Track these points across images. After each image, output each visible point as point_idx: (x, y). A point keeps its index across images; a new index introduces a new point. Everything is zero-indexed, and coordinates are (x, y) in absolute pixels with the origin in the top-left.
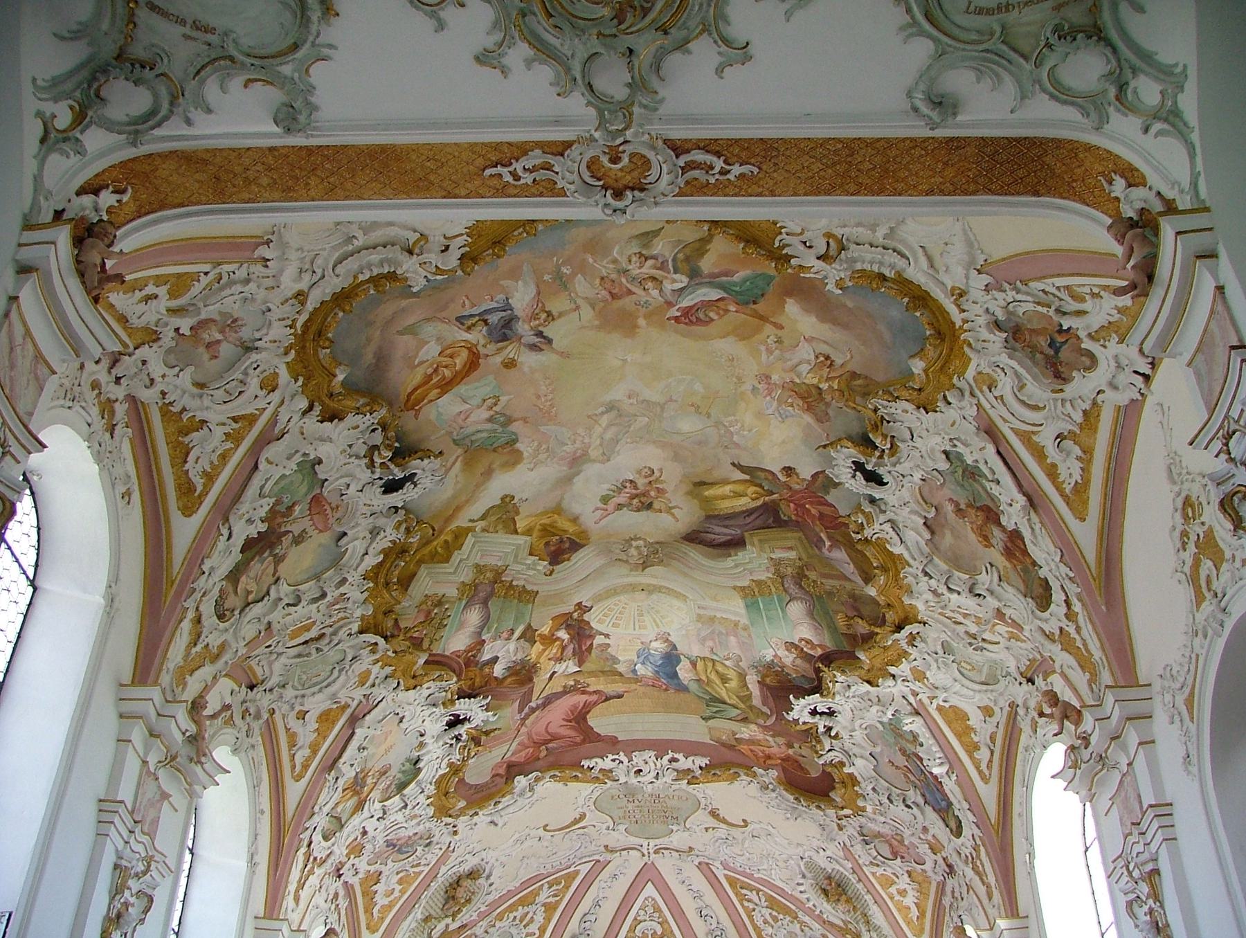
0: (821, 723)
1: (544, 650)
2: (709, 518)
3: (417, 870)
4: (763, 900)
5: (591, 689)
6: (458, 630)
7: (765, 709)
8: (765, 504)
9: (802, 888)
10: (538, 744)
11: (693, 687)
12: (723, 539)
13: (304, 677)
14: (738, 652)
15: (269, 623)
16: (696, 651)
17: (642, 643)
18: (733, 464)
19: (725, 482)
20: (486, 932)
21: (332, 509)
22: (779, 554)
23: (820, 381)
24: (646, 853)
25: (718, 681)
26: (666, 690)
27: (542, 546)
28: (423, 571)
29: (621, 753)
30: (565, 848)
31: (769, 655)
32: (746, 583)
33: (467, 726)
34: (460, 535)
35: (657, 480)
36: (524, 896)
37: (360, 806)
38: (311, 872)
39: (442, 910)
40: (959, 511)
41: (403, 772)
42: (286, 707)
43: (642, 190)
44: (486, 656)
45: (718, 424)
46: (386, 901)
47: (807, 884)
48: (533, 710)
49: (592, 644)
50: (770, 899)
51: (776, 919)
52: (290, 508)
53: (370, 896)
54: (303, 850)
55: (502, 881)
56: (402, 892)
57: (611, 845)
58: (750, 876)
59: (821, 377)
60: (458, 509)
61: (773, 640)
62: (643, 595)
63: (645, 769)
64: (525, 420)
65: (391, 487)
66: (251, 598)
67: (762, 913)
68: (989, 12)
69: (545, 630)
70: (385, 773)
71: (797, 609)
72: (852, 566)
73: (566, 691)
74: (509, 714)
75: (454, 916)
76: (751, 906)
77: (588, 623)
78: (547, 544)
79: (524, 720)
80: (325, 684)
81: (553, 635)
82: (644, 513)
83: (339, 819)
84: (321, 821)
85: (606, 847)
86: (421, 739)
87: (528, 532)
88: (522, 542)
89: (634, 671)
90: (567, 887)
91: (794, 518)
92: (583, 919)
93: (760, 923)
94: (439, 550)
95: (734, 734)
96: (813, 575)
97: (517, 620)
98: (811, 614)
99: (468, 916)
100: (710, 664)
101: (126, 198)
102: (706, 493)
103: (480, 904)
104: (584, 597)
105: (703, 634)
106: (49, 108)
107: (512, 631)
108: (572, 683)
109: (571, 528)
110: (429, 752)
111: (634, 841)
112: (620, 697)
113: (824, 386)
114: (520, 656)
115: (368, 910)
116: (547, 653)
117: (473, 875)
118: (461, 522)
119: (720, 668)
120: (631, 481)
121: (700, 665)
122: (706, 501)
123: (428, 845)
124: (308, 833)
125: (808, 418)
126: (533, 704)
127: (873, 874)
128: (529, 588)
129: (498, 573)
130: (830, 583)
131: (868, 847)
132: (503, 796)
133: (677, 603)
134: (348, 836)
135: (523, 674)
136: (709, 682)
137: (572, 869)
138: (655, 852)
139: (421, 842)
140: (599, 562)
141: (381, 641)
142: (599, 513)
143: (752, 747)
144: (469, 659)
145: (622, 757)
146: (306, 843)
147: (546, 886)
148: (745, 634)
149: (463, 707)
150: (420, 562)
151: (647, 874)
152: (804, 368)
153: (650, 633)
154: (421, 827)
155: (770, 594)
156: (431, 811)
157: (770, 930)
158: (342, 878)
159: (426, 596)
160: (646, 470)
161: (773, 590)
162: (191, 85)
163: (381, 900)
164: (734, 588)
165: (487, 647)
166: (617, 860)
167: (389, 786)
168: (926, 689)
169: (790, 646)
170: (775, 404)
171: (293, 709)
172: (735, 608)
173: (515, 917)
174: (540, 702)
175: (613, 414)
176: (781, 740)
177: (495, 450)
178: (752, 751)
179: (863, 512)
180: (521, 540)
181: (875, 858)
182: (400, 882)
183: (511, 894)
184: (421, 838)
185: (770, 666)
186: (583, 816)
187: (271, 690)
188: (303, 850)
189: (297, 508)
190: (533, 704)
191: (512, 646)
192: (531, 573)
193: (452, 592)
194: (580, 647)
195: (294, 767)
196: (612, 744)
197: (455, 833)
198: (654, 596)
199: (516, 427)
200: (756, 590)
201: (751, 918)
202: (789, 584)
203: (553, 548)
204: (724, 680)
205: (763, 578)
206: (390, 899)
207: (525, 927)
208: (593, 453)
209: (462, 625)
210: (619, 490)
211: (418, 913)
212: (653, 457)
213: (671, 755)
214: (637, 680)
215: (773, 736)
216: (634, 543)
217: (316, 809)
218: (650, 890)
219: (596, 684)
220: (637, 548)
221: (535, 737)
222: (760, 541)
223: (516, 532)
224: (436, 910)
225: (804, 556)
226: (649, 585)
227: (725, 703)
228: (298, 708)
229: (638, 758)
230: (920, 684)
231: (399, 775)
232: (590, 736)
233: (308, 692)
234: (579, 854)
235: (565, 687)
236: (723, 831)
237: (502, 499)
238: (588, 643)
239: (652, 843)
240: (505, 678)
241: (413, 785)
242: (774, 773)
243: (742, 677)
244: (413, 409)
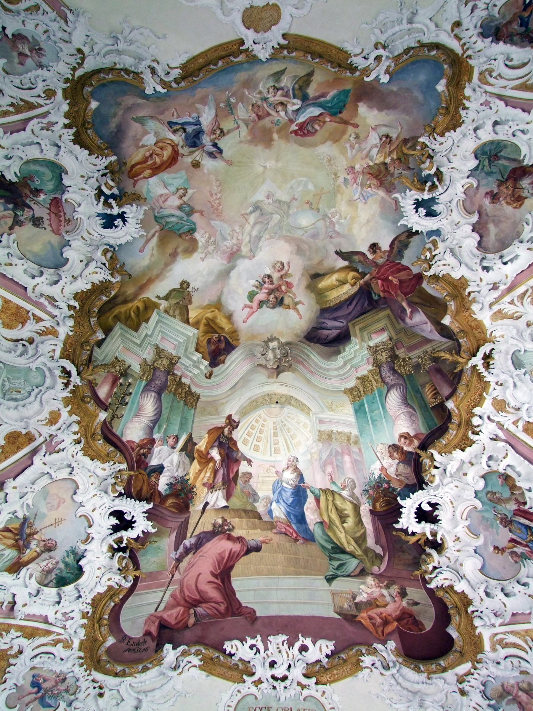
0: (426, 528)
1: (200, 471)
5: (236, 533)
6: (136, 415)
7: (379, 550)
8: (361, 288)
11: (317, 532)
12: (334, 333)
14: (351, 475)
17: (277, 472)
18: (337, 253)
19: (332, 271)
21: (66, 220)
23: (385, 158)
25: (337, 521)
26: (296, 540)
27: (205, 343)
29: (259, 637)
31: (375, 470)
32: (352, 383)
35: (286, 275)
40: (494, 197)
44: (154, 462)
48: (187, 551)
49: (237, 472)
59: (386, 153)
60: (150, 281)
61: (379, 449)
64: (202, 213)
72: (429, 323)
77: (235, 443)
78: (209, 341)
79: (179, 560)
81: (208, 453)
82: (278, 310)
88: (191, 334)
89: (270, 512)
91: (382, 295)
94: (132, 314)
96: (401, 353)
98: (405, 401)
100: (330, 498)
108: (220, 521)
114: (180, 473)
116: (202, 475)
119: (338, 502)
125: (381, 193)
126: (187, 542)
128: (194, 389)
133: (302, 418)
140: (246, 367)
142: (247, 310)
143: (370, 613)
144: (140, 455)
148: (355, 449)
152: (375, 151)
159: (116, 358)
160: (279, 264)
161: (374, 384)
164: (345, 392)
165: (156, 449)
168: (509, 416)
170: (360, 187)
174: (193, 541)
175: (258, 212)
176: (395, 589)
177: (180, 236)
178: (371, 618)
180: (191, 332)
185: (379, 483)
190: (187, 542)
192: (196, 371)
193: (136, 367)
199: (196, 217)
200: (361, 390)
203: (213, 347)
204: (343, 518)
205: (365, 372)
208: (245, 250)
210: (260, 286)
214: (272, 525)
215: (387, 587)
220: (273, 349)
221: (187, 593)
223: (187, 322)
225: (393, 334)
226: (282, 396)
227: (343, 551)
230: (504, 414)
231: (61, 565)
238: (235, 470)
240: (167, 496)
242: (392, 644)
243: (356, 508)
244: (133, 178)
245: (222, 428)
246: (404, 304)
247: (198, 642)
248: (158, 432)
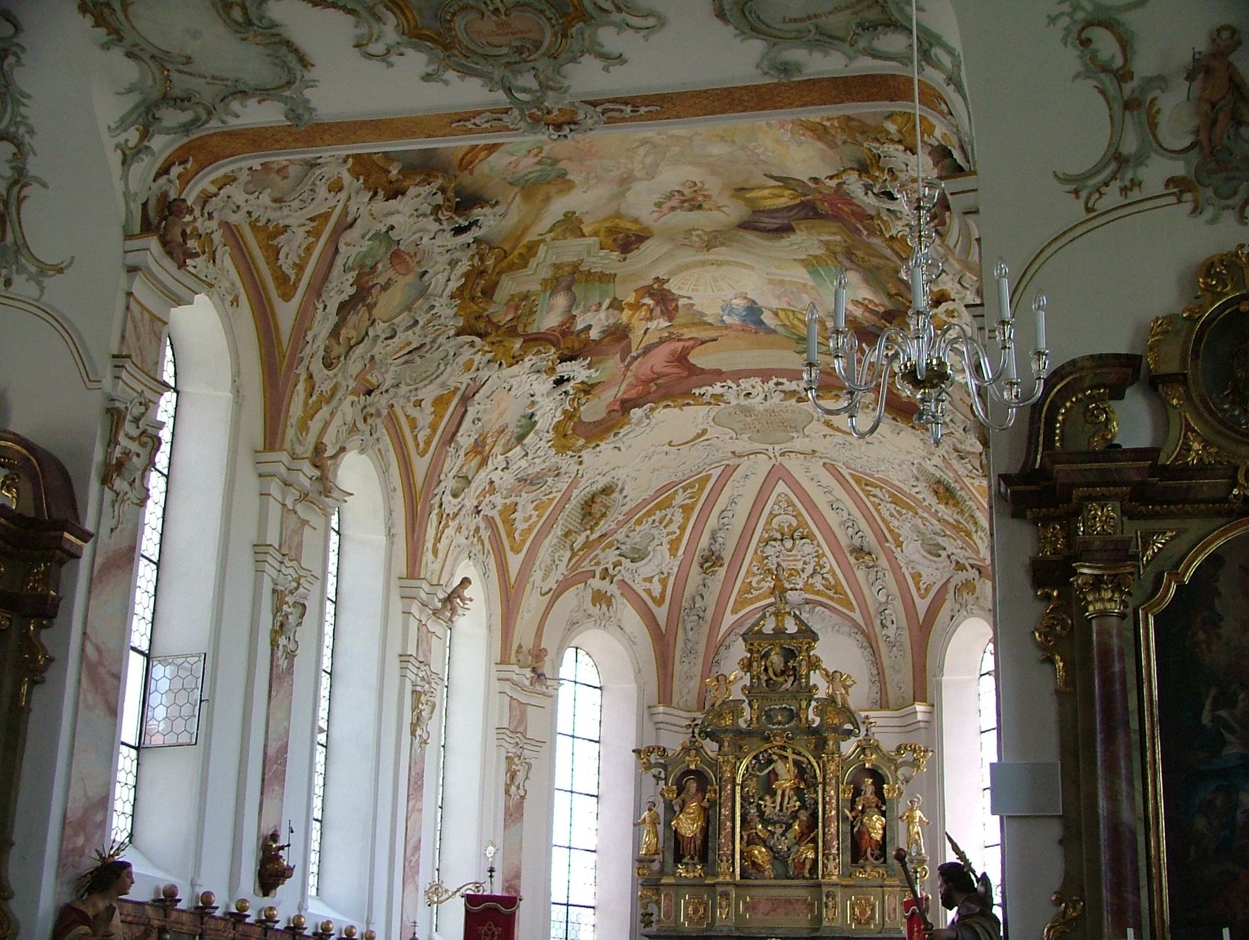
1: (633, 314)
2: (754, 212)
3: (550, 496)
4: (887, 496)
8: (802, 202)
9: (917, 490)
10: (647, 382)
11: (780, 329)
12: (774, 226)
13: (415, 375)
15: (373, 357)
16: (775, 304)
18: (766, 175)
19: (762, 188)
20: (627, 536)
22: (825, 238)
24: (772, 456)
28: (505, 279)
30: (693, 458)
32: (804, 257)
33: (572, 383)
34: (532, 248)
35: (701, 190)
36: (661, 500)
37: (484, 462)
38: (447, 526)
39: (581, 524)
41: (521, 426)
42: (402, 401)
43: (575, 123)
45: (743, 148)
46: (526, 526)
47: (921, 486)
48: (635, 358)
49: (677, 305)
50: (892, 495)
51: (900, 514)
52: (374, 268)
53: (509, 523)
54: (435, 511)
55: (635, 491)
56: (539, 516)
57: (738, 450)
58: (872, 476)
60: (526, 229)
62: (714, 267)
63: (754, 392)
64: (570, 159)
65: (459, 231)
66: (352, 343)
67: (887, 508)
68: (801, 20)
69: (631, 299)
70: (503, 431)
71: (853, 277)
73: (662, 341)
74: (613, 364)
75: (592, 529)
76: (877, 501)
77: (669, 291)
78: (615, 240)
80: (434, 376)
83: (466, 478)
84: (449, 483)
85: (733, 453)
86: (533, 399)
87: (596, 234)
89: (723, 321)
90: (702, 489)
92: (721, 516)
93: (887, 516)
95: (828, 365)
97: (603, 296)
98: (866, 281)
99: (606, 526)
101: (189, 166)
102: (748, 196)
103: (616, 515)
104: (661, 272)
105: (778, 292)
106: (121, 139)
107: (600, 305)
109: (634, 227)
110: (541, 407)
111: (757, 446)
112: (715, 340)
113: (828, 124)
114: (611, 321)
115: (510, 535)
116: (636, 316)
117: (607, 491)
118: (531, 237)
119: (800, 316)
120: (678, 191)
121: (781, 314)
122: (750, 202)
123: (557, 475)
124: (438, 497)
125: (820, 145)
126: (634, 354)
127: (972, 484)
129: (575, 267)
130: (875, 261)
131: (964, 461)
132: (621, 428)
134: (477, 488)
135: (619, 334)
136: (794, 326)
137: (704, 474)
138: (782, 455)
139: (550, 473)
140: (666, 248)
141: (477, 339)
145: (730, 383)
146: (437, 505)
147: (681, 490)
148: (813, 292)
149: (564, 369)
150: (500, 273)
151: (776, 474)
153: (728, 294)
154: (547, 464)
155: (827, 264)
156: (553, 451)
157: (896, 523)
158: (482, 513)
162: (220, 106)
163: (520, 526)
165: (579, 320)
166: (745, 463)
167: (509, 440)
169: (856, 303)
170: (789, 135)
171: (409, 401)
172: (801, 275)
173: (654, 521)
175: (648, 147)
177: (549, 183)
179: (882, 220)
180: (591, 240)
181: (971, 471)
182: (536, 509)
183: (646, 502)
184: (550, 470)
186: (704, 432)
187: (387, 391)
188: (435, 511)
189: (380, 266)
191: (602, 315)
194: (667, 308)
195: (417, 445)
196: (718, 375)
197: (581, 463)
198: (725, 268)
199: (562, 165)
201: (878, 511)
202: (840, 257)
206: (528, 524)
207: (665, 527)
209: (551, 309)
211: (558, 531)
212: (694, 174)
213: (775, 380)
214: (727, 327)
216: (694, 233)
217: (442, 477)
218: (781, 487)
219: (688, 333)
220: (697, 236)
222: (807, 228)
223: (584, 236)
224: (575, 524)
228: (413, 399)
229: (745, 384)
232: (693, 371)
233: (420, 385)
234: (708, 461)
235: (660, 338)
236: (839, 437)
237: (565, 215)
238: (674, 305)
239: (777, 447)
241: (531, 435)
245: (651, 286)
246: (859, 226)
247: (664, 397)
248: (577, 308)
